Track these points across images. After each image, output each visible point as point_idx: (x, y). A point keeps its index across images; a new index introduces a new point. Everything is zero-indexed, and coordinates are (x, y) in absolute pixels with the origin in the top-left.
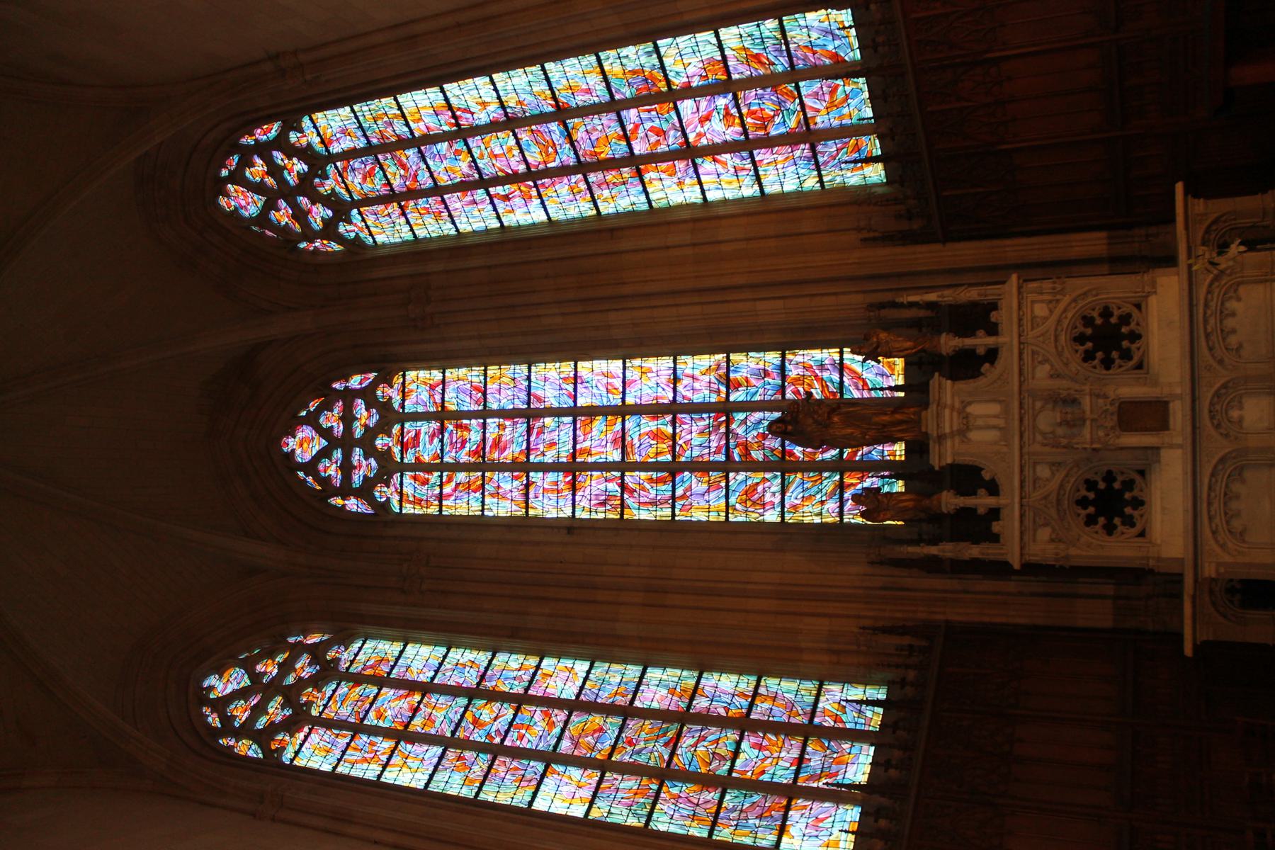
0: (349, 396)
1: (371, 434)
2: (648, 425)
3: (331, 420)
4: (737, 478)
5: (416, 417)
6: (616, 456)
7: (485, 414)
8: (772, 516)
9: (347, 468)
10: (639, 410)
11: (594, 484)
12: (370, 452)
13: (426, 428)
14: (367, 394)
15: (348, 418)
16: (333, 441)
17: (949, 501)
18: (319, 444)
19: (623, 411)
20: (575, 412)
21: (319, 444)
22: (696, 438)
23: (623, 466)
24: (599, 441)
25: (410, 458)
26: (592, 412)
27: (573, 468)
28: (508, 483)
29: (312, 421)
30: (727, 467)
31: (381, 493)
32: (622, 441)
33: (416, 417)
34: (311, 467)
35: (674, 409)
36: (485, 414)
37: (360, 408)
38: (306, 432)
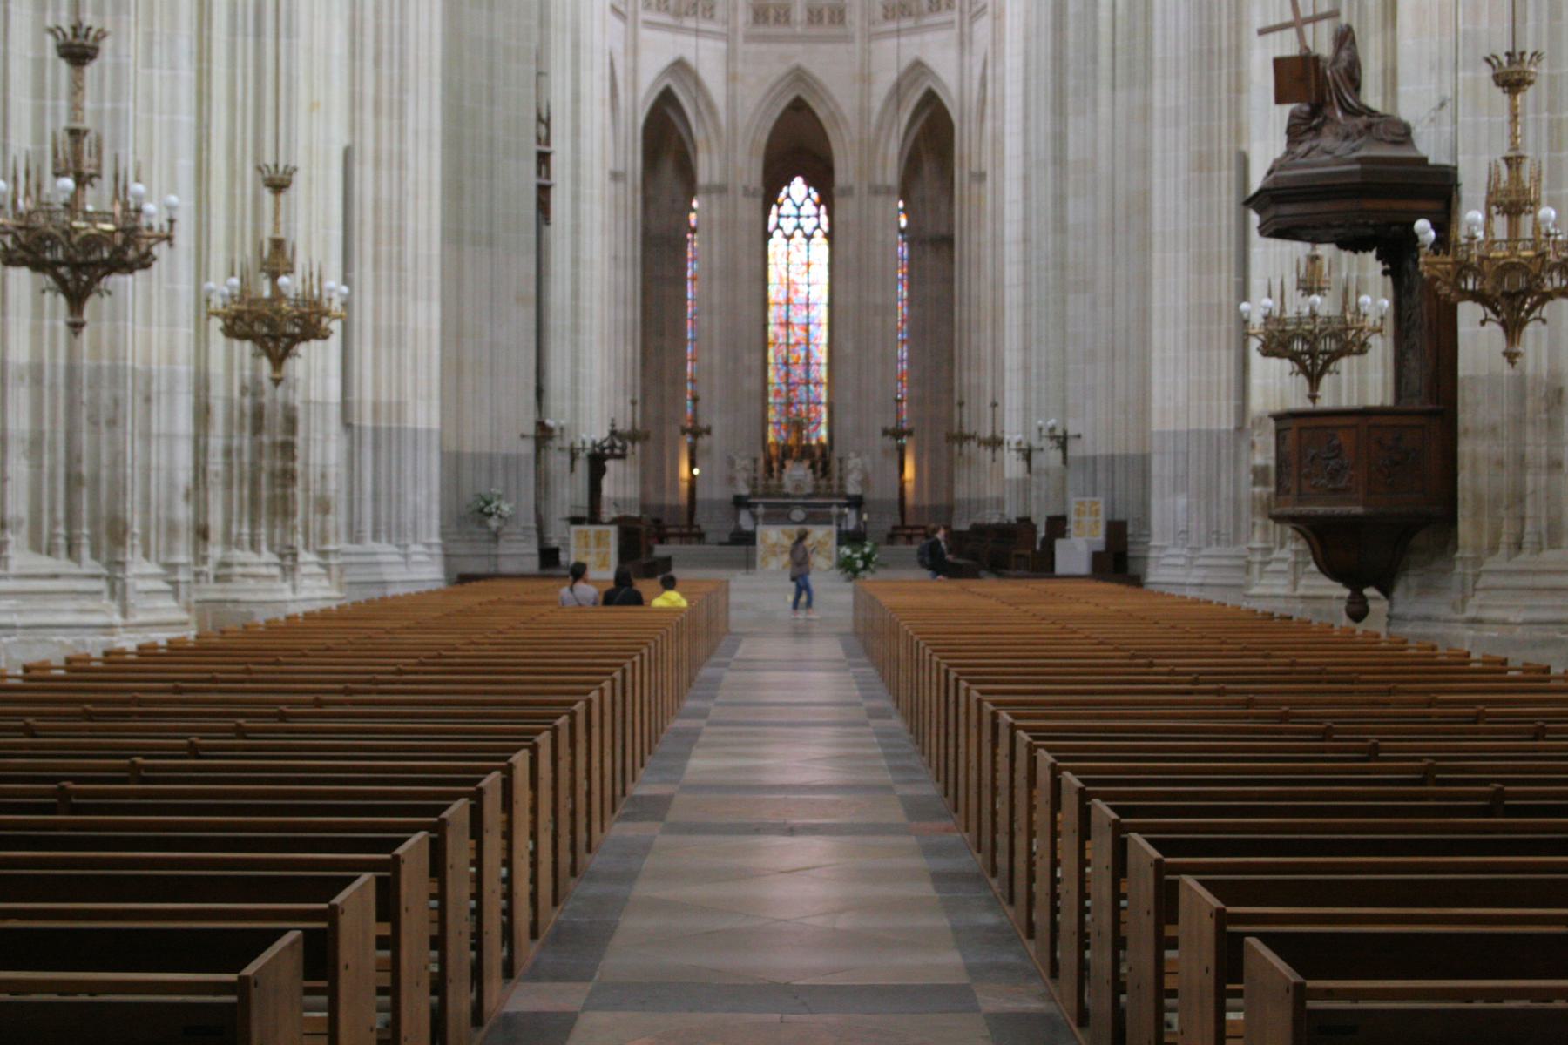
0: (818, 216)
2: (802, 354)
3: (809, 208)
4: (784, 388)
6: (792, 341)
8: (771, 400)
10: (808, 352)
11: (782, 331)
14: (818, 227)
17: (775, 465)
19: (808, 343)
20: (808, 325)
22: (798, 373)
23: (788, 345)
24: (797, 334)
25: (792, 248)
26: (807, 331)
27: (787, 324)
28: (782, 298)
29: (809, 196)
30: (788, 384)
31: (777, 234)
32: (798, 343)
34: (788, 196)
35: (808, 364)
37: (814, 222)
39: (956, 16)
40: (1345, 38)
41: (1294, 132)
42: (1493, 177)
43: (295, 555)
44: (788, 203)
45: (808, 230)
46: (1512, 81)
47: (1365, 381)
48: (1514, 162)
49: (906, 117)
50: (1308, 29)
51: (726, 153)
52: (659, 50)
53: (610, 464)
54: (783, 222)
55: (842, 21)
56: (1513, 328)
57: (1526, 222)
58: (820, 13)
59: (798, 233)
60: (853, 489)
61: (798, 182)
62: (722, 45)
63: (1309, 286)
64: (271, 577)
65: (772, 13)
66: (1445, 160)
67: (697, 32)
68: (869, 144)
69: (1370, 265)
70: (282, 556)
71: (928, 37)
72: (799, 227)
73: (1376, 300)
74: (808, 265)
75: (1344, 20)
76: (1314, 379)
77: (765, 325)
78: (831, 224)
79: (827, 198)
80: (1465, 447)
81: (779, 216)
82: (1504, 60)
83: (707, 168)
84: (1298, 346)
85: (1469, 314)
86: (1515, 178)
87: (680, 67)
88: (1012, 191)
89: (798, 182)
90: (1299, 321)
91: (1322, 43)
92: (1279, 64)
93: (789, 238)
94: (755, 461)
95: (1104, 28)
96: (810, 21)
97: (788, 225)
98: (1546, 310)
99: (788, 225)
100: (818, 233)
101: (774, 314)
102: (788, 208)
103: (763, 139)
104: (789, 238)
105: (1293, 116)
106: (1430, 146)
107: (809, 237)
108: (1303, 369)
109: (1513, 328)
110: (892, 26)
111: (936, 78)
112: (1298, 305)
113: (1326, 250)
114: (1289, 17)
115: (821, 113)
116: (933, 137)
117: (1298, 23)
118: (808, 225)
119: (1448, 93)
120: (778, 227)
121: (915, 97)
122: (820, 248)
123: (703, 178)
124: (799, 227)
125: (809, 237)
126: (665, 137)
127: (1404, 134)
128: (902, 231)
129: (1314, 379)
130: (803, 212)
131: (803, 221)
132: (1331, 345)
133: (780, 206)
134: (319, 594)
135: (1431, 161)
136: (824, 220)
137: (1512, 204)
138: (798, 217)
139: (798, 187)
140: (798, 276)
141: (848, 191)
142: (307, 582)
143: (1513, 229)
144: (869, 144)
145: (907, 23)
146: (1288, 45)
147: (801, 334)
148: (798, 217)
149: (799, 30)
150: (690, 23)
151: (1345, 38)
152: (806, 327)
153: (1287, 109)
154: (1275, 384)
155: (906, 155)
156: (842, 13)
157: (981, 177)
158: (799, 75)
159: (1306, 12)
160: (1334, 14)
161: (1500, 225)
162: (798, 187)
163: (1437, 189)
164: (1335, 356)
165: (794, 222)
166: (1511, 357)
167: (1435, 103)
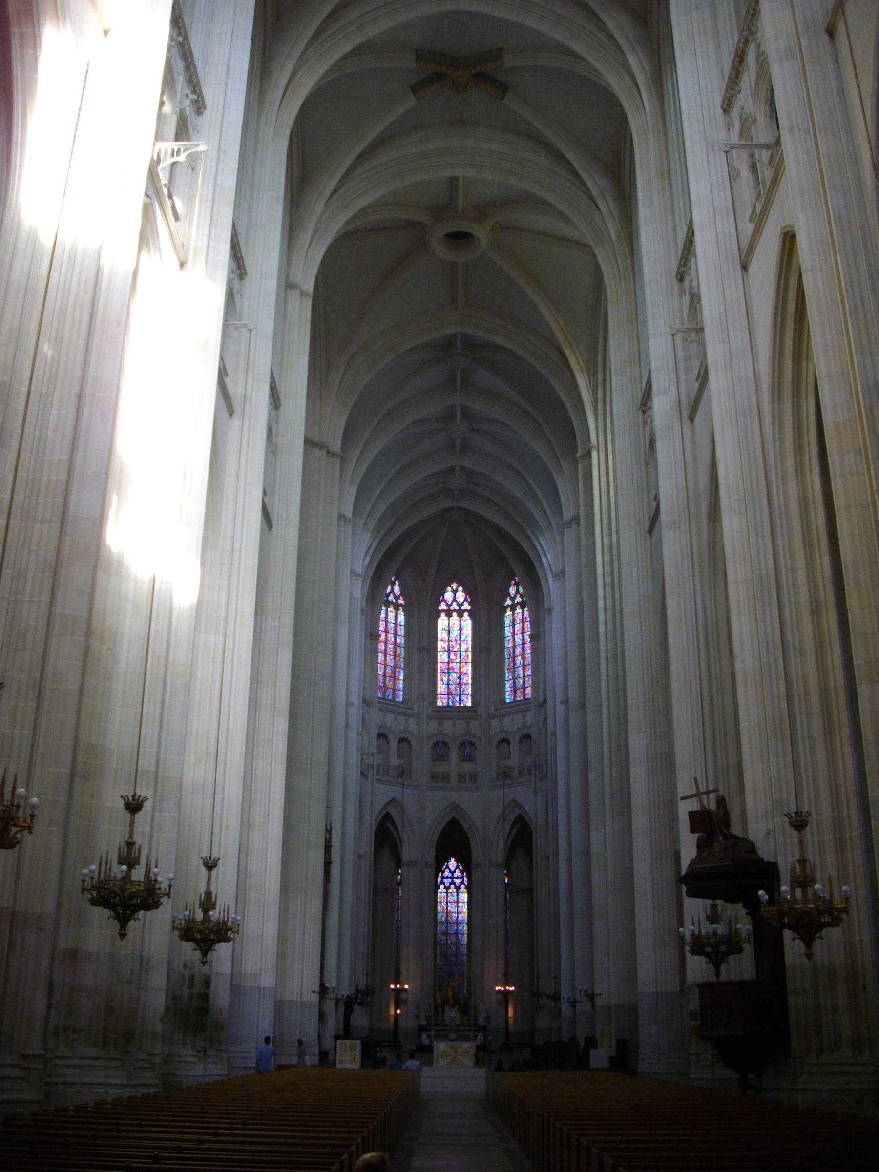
0: (462, 877)
1: (454, 884)
3: (458, 873)
5: (457, 895)
7: (458, 913)
9: (447, 877)
12: (451, 884)
13: (455, 898)
14: (462, 883)
15: (457, 878)
16: (453, 873)
18: (452, 869)
21: (452, 869)
27: (446, 933)
29: (457, 867)
31: (442, 886)
33: (457, 895)
34: (448, 867)
36: (458, 913)
38: (455, 864)
39: (533, 779)
40: (721, 802)
41: (700, 846)
42: (794, 870)
43: (205, 1052)
44: (447, 870)
45: (457, 885)
46: (799, 823)
47: (741, 967)
48: (803, 862)
49: (507, 829)
50: (705, 797)
51: (416, 846)
52: (383, 794)
53: (356, 1007)
54: (445, 880)
55: (475, 780)
56: (808, 942)
57: (810, 891)
58: (464, 776)
59: (452, 886)
60: (481, 1022)
61: (453, 859)
62: (415, 792)
63: (713, 918)
64: (193, 1062)
65: (440, 776)
66: (772, 860)
67: (403, 785)
68: (489, 841)
69: (740, 910)
70: (198, 1052)
71: (518, 788)
72: (452, 883)
73: (744, 926)
74: (457, 902)
75: (721, 793)
76: (717, 967)
77: (436, 933)
78: (469, 881)
79: (467, 866)
80: (791, 1000)
81: (443, 877)
82: (793, 815)
83: (408, 852)
84: (708, 949)
85: (787, 934)
86: (803, 870)
87: (393, 800)
88: (563, 867)
89: (453, 859)
90: (708, 936)
91: (711, 804)
92: (692, 814)
93: (447, 888)
94: (430, 1006)
95: (607, 788)
96: (460, 780)
97: (447, 882)
98: (824, 932)
99: (447, 882)
100: (463, 886)
101: (440, 927)
102: (447, 873)
103: (435, 838)
104: (447, 888)
105: (699, 839)
106: (765, 852)
107: (458, 888)
108: (711, 961)
109: (808, 942)
110: (501, 783)
111: (523, 808)
112: (707, 929)
113: (720, 902)
114: (694, 792)
115: (465, 826)
116: (522, 837)
117: (698, 795)
118: (458, 881)
119: (771, 828)
120: (442, 883)
121: (512, 818)
122: (464, 896)
123: (406, 857)
124: (452, 883)
125: (458, 888)
126: (386, 836)
127: (751, 847)
128: (506, 885)
129: (717, 967)
130: (455, 875)
131: (455, 880)
132: (723, 948)
133: (443, 872)
134: (216, 1073)
135: (765, 860)
136: (465, 879)
137: (803, 881)
138: (452, 878)
139: (452, 864)
140: (452, 908)
141: (479, 865)
142: (210, 1066)
143: (804, 894)
144: (489, 841)
145: (506, 782)
146: (693, 805)
147: (453, 938)
148: (452, 878)
149: (454, 784)
150: (400, 780)
151: (721, 802)
152: (457, 934)
153: (697, 835)
154: (697, 967)
155: (508, 846)
156: (475, 776)
157: (547, 858)
158: (454, 807)
159: (703, 788)
160: (715, 790)
161: (799, 892)
162: (452, 864)
163: (768, 873)
164: (727, 954)
165: (450, 880)
166: (809, 956)
167: (765, 832)
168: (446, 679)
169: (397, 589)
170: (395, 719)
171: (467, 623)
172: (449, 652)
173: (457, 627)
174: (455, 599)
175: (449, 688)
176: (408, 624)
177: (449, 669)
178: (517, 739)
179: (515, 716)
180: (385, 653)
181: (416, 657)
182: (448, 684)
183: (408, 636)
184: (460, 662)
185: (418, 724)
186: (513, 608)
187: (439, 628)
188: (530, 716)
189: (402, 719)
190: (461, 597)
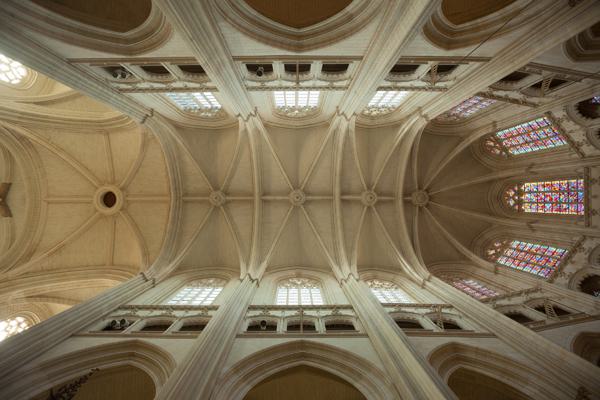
168: (565, 205)
169: (497, 245)
170: (573, 263)
171: (528, 186)
172: (545, 202)
173: (528, 195)
174: (513, 197)
175: (571, 203)
176: (521, 239)
177: (557, 203)
178: (589, 122)
179: (568, 130)
180: (528, 263)
181: (538, 234)
182: (568, 203)
183: (527, 240)
184: (552, 192)
185: (592, 238)
186: (505, 149)
187: (529, 211)
188: (559, 114)
189: (576, 257)
190: (512, 193)
